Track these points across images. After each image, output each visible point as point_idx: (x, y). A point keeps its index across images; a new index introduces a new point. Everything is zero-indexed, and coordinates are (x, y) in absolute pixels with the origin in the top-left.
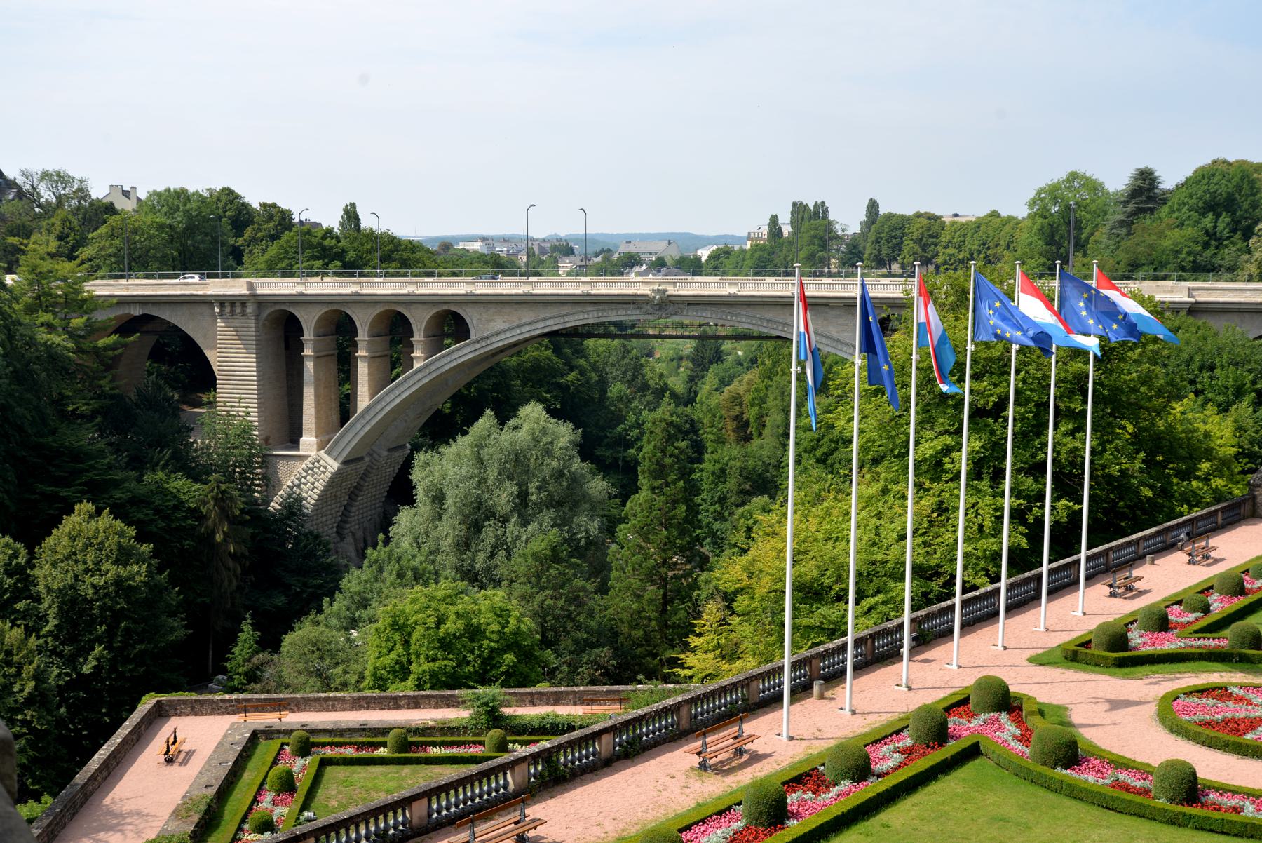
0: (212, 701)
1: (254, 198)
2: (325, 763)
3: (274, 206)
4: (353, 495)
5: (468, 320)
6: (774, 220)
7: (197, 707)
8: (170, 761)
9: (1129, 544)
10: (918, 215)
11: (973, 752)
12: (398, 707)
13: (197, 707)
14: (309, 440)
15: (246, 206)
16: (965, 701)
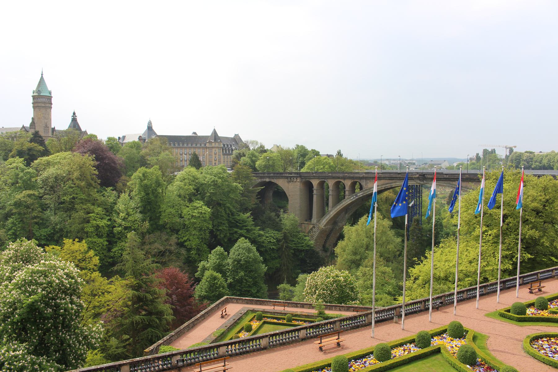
0: (242, 299)
1: (309, 148)
2: (265, 323)
3: (314, 150)
4: (328, 236)
5: (362, 184)
6: (478, 154)
7: (238, 301)
8: (222, 317)
9: (548, 271)
10: (526, 152)
11: (438, 351)
12: (297, 307)
13: (238, 301)
14: (314, 220)
15: (307, 150)
16: (445, 331)
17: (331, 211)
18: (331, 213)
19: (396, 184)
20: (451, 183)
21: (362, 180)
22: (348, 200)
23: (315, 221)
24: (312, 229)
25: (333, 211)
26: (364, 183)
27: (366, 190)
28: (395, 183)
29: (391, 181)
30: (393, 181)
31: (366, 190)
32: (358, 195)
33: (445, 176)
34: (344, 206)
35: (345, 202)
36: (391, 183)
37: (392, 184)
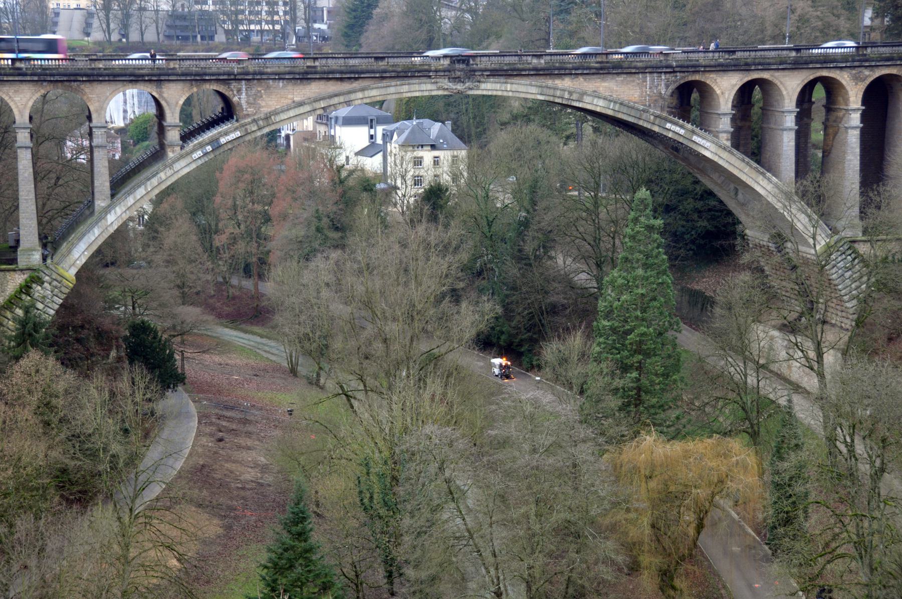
5: (235, 99)
17: (107, 210)
18: (111, 218)
19: (367, 93)
20: (550, 82)
21: (234, 85)
22: (183, 163)
23: (37, 257)
24: (26, 289)
25: (119, 210)
26: (244, 96)
27: (254, 121)
28: (363, 90)
29: (346, 86)
30: (356, 85)
31: (254, 121)
32: (223, 140)
33: (535, 61)
34: (163, 187)
35: (169, 172)
36: (350, 92)
37: (353, 96)
